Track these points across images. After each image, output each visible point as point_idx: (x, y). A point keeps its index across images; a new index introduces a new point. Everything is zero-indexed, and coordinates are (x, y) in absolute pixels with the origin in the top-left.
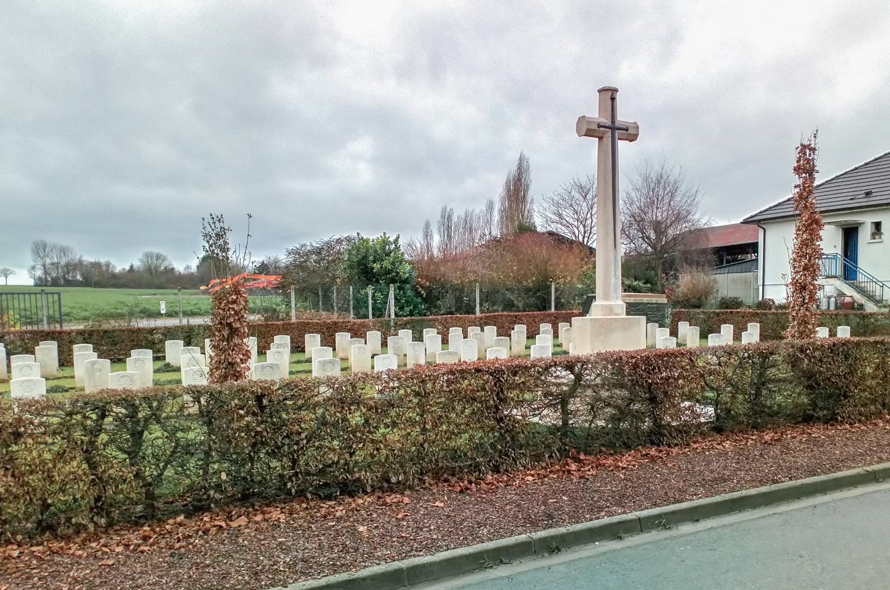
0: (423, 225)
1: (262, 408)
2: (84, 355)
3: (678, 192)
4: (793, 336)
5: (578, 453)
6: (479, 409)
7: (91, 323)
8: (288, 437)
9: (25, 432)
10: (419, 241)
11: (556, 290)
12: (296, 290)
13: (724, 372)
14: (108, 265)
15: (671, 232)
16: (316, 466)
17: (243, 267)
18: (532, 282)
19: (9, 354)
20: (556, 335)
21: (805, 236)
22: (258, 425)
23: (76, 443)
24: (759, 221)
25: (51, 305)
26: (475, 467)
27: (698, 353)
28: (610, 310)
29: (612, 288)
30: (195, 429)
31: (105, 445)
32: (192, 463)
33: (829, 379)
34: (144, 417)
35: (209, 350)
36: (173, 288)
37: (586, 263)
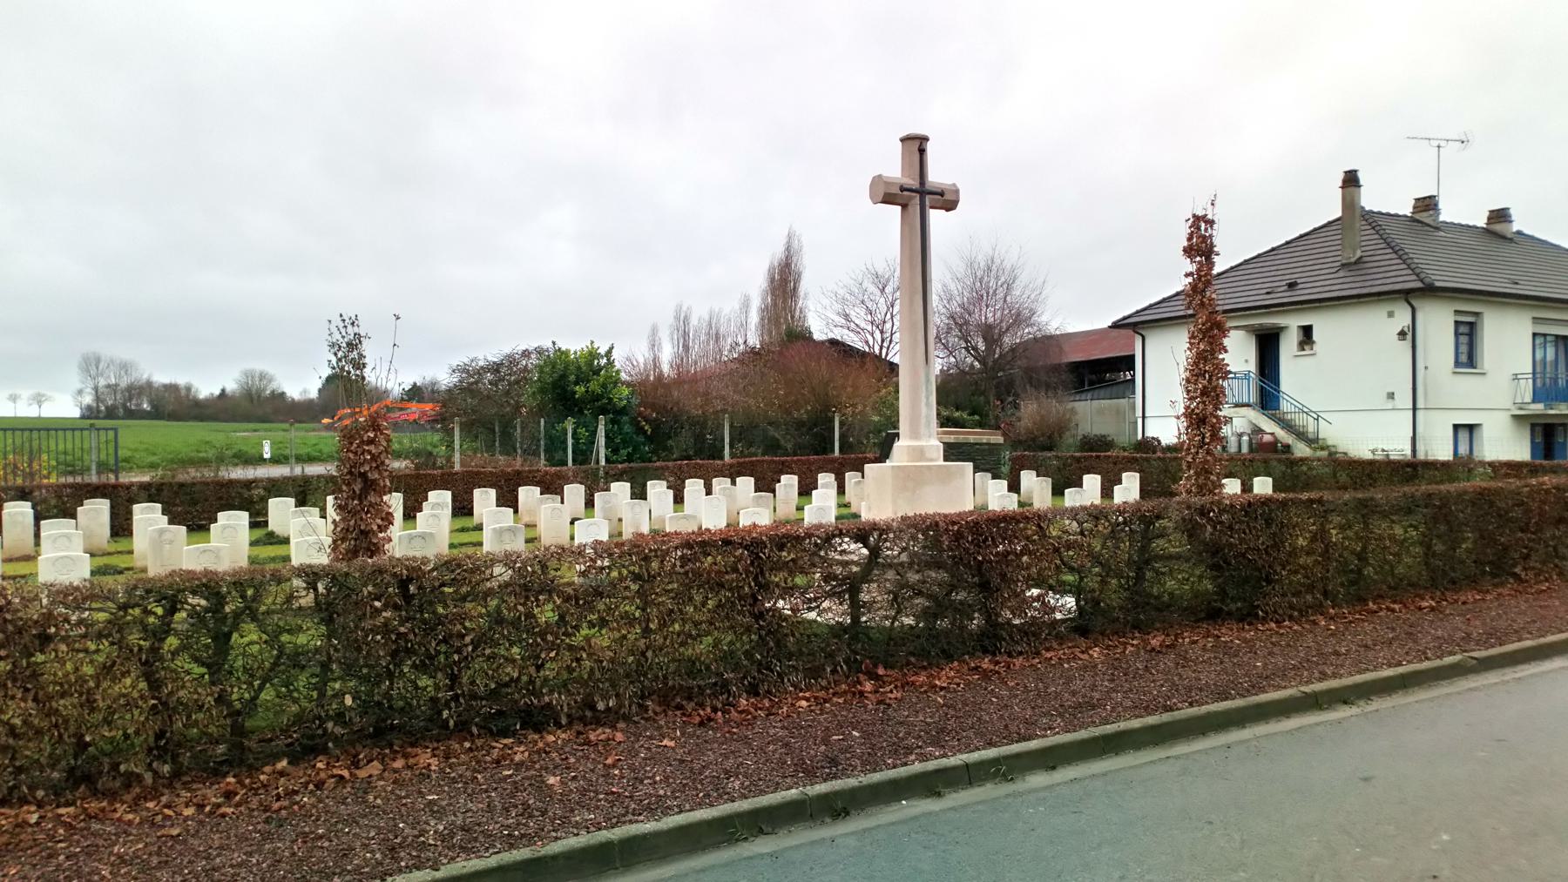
0: (647, 331)
1: (408, 598)
2: (148, 518)
4: (1189, 492)
5: (876, 666)
6: (728, 599)
7: (160, 472)
8: (445, 641)
9: (56, 634)
10: (642, 355)
11: (842, 424)
14: (188, 389)
15: (1007, 340)
17: (386, 391)
18: (807, 412)
19: (38, 518)
20: (841, 490)
24: (1135, 325)
28: (920, 453)
29: (923, 421)
31: (175, 653)
32: (302, 681)
33: (1243, 555)
35: (331, 512)
37: (885, 385)
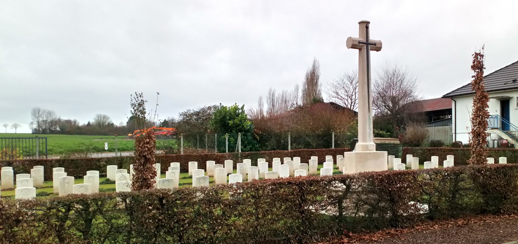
0: (258, 99)
1: (162, 205)
2: (59, 173)
3: (405, 80)
4: (474, 163)
5: (349, 232)
6: (290, 206)
7: (64, 155)
8: (177, 222)
9: (22, 219)
10: (255, 109)
11: (335, 136)
12: (184, 136)
13: (434, 184)
14: (75, 122)
15: (401, 103)
16: (194, 240)
17: (154, 123)
18: (321, 131)
19: (15, 173)
20: (335, 162)
21: (479, 105)
22: (160, 215)
23: (52, 226)
24: (452, 96)
25: (41, 145)
26: (287, 241)
27: (418, 172)
28: (366, 147)
29: (368, 135)
30: (123, 218)
31: (69, 227)
32: (120, 238)
33: (495, 188)
34: (93, 210)
35: (132, 171)
36: (112, 135)
37: (352, 121)
